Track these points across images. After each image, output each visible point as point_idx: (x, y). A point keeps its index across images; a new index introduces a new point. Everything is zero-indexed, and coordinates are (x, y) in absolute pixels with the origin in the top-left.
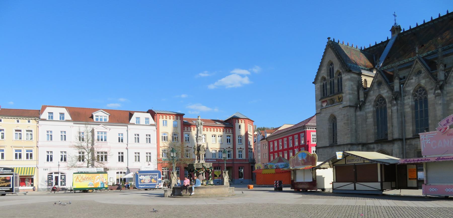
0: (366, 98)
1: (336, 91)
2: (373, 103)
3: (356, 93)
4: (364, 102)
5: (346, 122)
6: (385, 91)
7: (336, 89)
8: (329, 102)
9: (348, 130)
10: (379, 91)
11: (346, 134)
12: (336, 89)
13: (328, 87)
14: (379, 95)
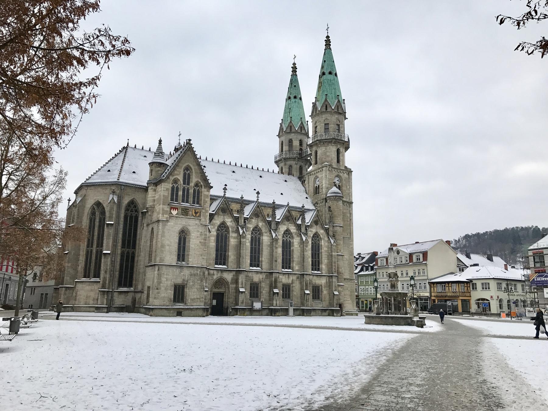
2: (216, 228)
5: (202, 241)
11: (201, 255)
13: (180, 193)
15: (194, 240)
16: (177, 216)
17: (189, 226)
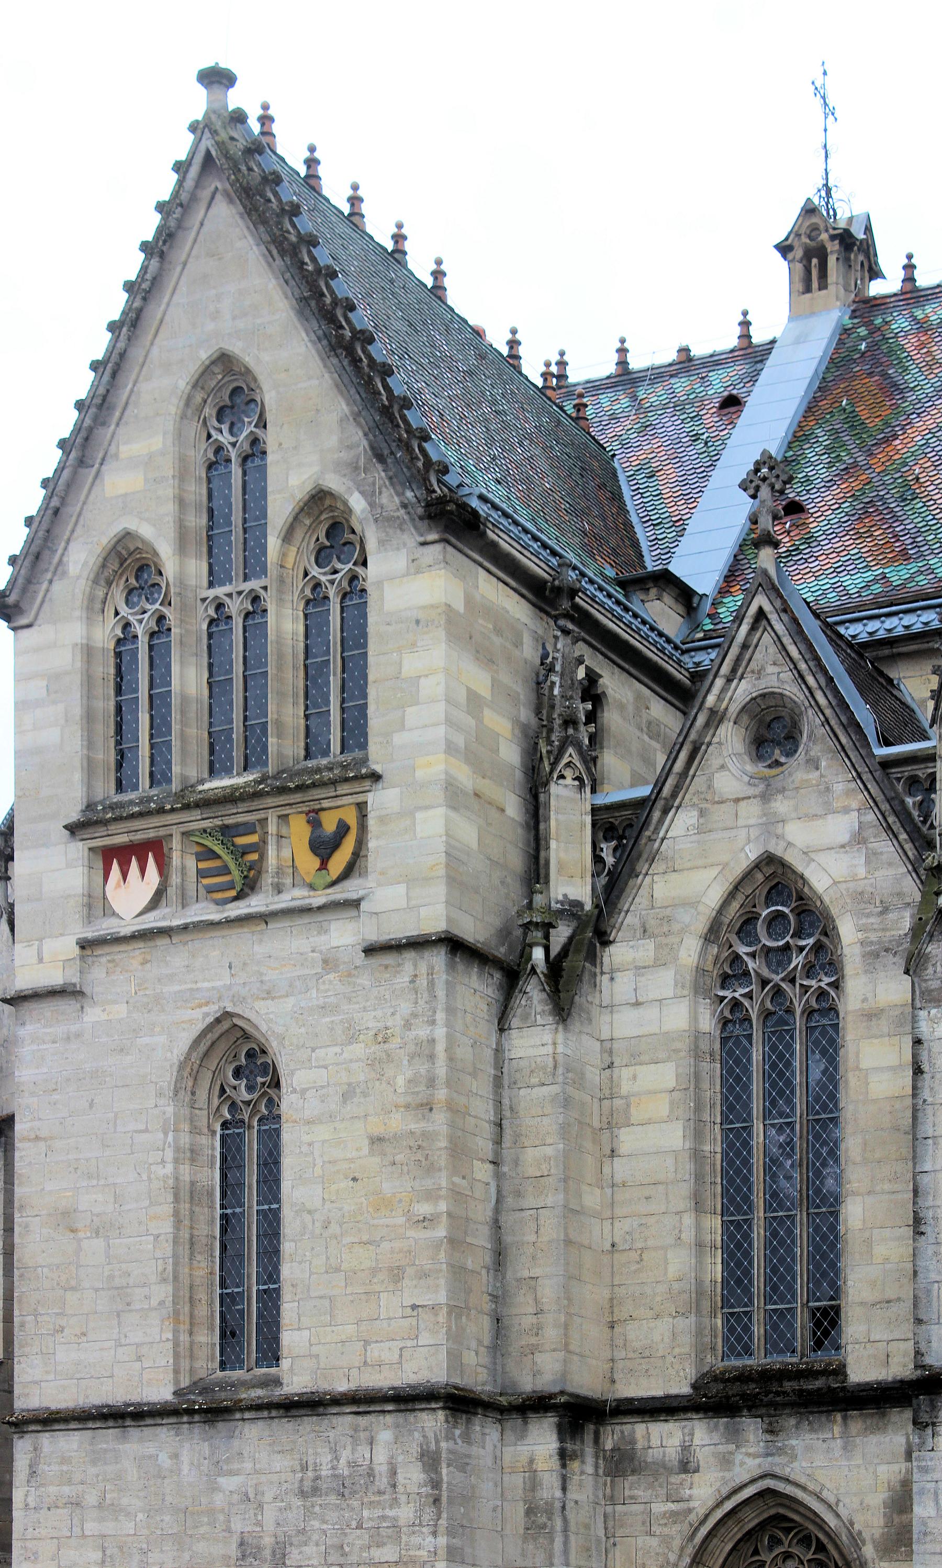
0: (614, 884)
1: (285, 747)
2: (690, 951)
3: (514, 808)
4: (595, 929)
5: (398, 1122)
6: (840, 827)
7: (285, 713)
8: (183, 859)
9: (426, 1221)
10: (771, 824)
11: (397, 1275)
12: (285, 713)
13: (188, 678)
14: (769, 861)
15: (322, 1133)
16: (153, 920)
17: (269, 995)
